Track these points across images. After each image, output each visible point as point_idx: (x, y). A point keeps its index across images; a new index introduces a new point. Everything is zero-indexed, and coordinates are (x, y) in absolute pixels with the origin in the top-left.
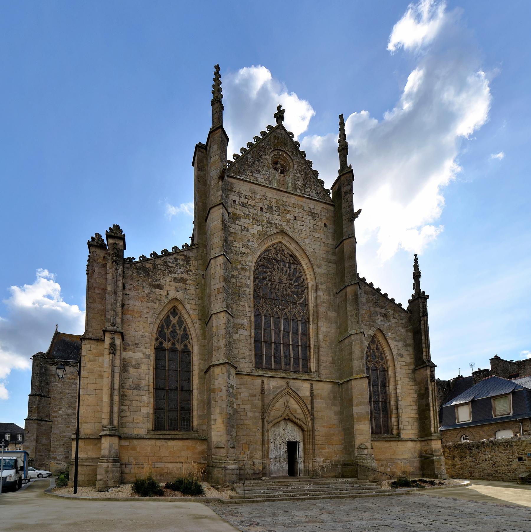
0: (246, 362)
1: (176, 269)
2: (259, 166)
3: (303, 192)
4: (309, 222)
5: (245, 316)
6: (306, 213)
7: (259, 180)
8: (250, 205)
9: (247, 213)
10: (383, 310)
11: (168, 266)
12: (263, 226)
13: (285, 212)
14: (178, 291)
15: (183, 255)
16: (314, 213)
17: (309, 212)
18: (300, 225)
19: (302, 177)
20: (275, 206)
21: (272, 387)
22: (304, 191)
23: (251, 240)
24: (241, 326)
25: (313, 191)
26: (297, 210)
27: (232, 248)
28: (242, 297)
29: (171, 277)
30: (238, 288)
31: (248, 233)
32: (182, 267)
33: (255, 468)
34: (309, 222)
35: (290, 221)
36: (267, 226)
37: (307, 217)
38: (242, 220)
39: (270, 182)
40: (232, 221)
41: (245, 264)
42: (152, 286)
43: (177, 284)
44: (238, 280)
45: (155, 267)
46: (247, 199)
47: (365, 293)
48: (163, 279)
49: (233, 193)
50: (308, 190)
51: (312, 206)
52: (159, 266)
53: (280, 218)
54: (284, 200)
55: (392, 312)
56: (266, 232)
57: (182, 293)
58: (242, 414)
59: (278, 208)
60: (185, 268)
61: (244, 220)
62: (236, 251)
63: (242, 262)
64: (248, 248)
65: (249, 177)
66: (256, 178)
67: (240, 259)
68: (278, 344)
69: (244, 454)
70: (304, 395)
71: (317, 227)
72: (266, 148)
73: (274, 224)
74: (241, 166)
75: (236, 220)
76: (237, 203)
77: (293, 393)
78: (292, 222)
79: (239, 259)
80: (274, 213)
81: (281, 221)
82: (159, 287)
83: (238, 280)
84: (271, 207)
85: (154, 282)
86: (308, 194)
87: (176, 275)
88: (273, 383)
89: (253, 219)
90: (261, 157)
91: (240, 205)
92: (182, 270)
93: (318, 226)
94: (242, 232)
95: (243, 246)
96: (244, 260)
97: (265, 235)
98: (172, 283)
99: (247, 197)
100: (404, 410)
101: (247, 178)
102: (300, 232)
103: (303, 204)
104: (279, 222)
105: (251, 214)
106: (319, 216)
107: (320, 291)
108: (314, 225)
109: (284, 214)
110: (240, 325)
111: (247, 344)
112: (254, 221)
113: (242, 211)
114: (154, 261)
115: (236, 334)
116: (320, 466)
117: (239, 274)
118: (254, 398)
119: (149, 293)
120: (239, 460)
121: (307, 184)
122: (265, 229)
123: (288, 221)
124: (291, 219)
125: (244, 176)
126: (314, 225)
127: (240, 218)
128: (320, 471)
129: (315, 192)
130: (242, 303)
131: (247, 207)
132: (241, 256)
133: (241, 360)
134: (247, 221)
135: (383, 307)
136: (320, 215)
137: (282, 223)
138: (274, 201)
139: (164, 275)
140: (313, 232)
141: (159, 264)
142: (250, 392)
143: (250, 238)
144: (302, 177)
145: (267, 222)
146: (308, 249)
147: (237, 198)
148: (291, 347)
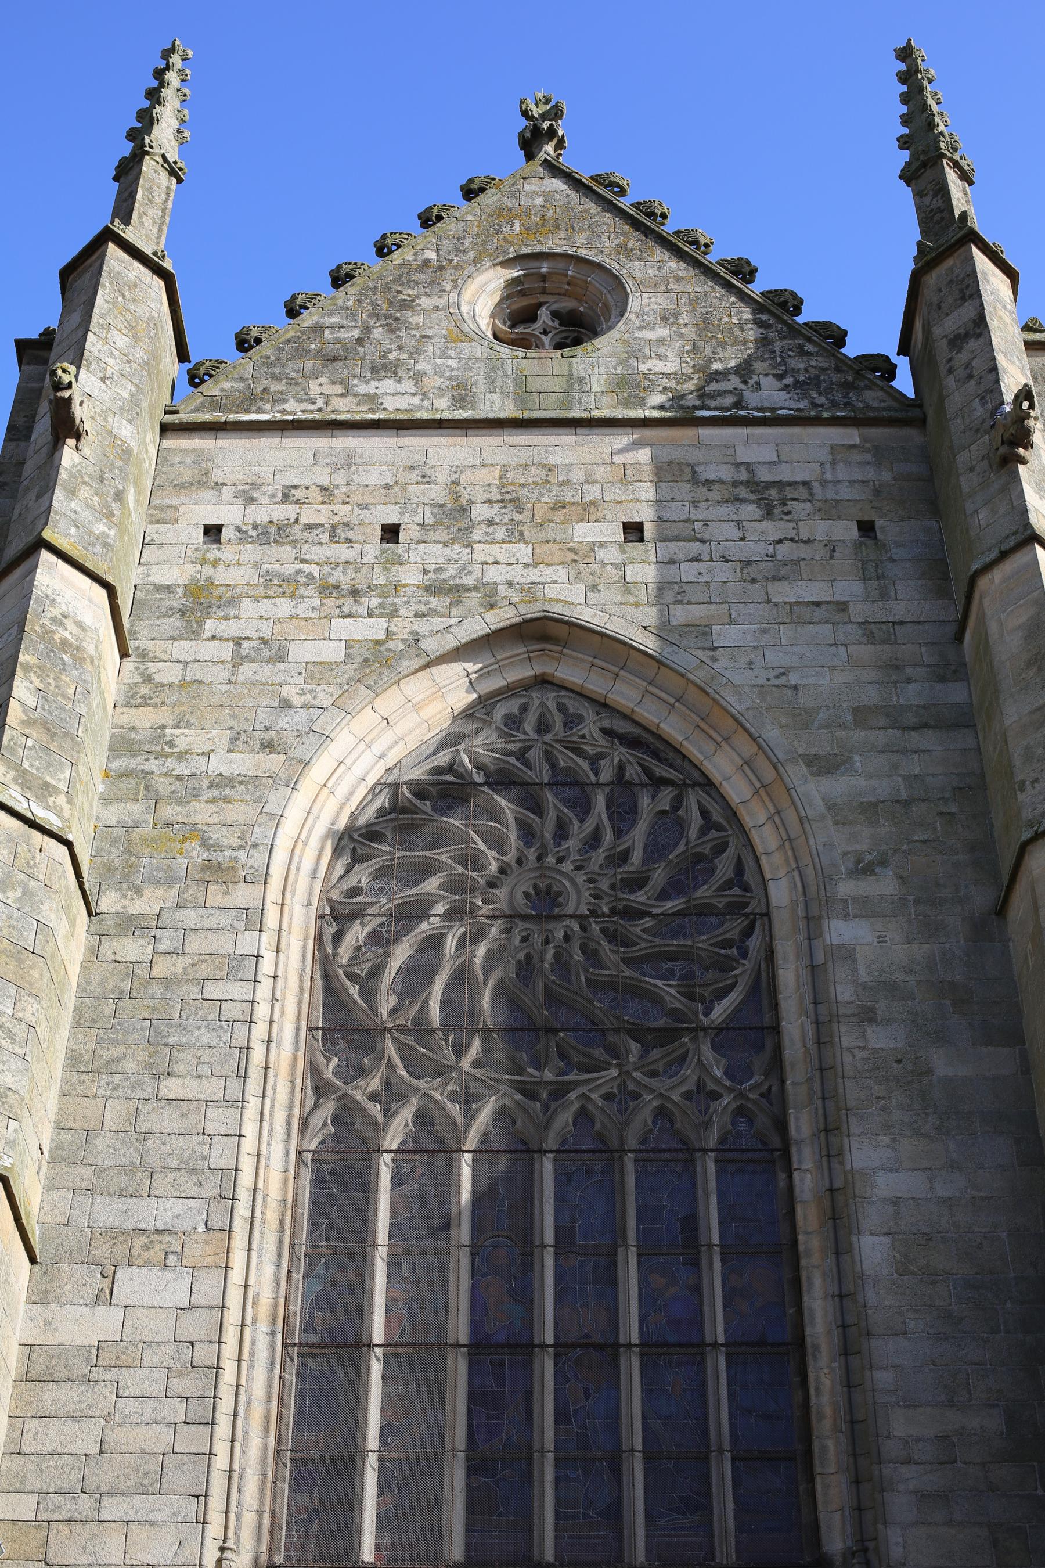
0: (158, 1517)
2: (394, 346)
4: (736, 534)
5: (193, 1172)
6: (715, 495)
7: (390, 403)
8: (310, 527)
9: (289, 569)
12: (393, 614)
13: (559, 515)
16: (780, 485)
17: (736, 484)
20: (489, 502)
23: (297, 701)
24: (146, 1248)
25: (768, 382)
27: (153, 765)
30: (157, 990)
31: (282, 666)
34: (736, 534)
35: (600, 554)
36: (423, 608)
37: (725, 510)
40: (174, 628)
41: (236, 842)
44: (165, 945)
46: (297, 502)
49: (209, 494)
53: (524, 552)
54: (556, 458)
56: (417, 638)
61: (265, 607)
62: (179, 778)
63: (217, 835)
64: (269, 746)
65: (320, 403)
67: (202, 813)
71: (803, 551)
72: (441, 268)
73: (476, 588)
74: (276, 370)
78: (611, 555)
79: (198, 819)
80: (477, 534)
81: (526, 565)
83: (165, 945)
84: (463, 510)
86: (729, 401)
89: (327, 589)
93: (808, 542)
95: (234, 740)
96: (230, 819)
99: (299, 494)
103: (694, 456)
104: (517, 574)
107: (846, 917)
108: (780, 541)
110: (139, 1243)
111: (182, 1372)
112: (330, 602)
113: (257, 565)
115: (101, 1310)
122: (403, 627)
124: (602, 545)
125: (291, 405)
126: (780, 541)
127: (234, 601)
129: (779, 385)
130: (172, 1087)
131: (294, 543)
133: (113, 1509)
134: (284, 607)
136: (823, 483)
137: (533, 575)
140: (776, 578)
143: (289, 692)
145: (427, 589)
148: (632, 1367)
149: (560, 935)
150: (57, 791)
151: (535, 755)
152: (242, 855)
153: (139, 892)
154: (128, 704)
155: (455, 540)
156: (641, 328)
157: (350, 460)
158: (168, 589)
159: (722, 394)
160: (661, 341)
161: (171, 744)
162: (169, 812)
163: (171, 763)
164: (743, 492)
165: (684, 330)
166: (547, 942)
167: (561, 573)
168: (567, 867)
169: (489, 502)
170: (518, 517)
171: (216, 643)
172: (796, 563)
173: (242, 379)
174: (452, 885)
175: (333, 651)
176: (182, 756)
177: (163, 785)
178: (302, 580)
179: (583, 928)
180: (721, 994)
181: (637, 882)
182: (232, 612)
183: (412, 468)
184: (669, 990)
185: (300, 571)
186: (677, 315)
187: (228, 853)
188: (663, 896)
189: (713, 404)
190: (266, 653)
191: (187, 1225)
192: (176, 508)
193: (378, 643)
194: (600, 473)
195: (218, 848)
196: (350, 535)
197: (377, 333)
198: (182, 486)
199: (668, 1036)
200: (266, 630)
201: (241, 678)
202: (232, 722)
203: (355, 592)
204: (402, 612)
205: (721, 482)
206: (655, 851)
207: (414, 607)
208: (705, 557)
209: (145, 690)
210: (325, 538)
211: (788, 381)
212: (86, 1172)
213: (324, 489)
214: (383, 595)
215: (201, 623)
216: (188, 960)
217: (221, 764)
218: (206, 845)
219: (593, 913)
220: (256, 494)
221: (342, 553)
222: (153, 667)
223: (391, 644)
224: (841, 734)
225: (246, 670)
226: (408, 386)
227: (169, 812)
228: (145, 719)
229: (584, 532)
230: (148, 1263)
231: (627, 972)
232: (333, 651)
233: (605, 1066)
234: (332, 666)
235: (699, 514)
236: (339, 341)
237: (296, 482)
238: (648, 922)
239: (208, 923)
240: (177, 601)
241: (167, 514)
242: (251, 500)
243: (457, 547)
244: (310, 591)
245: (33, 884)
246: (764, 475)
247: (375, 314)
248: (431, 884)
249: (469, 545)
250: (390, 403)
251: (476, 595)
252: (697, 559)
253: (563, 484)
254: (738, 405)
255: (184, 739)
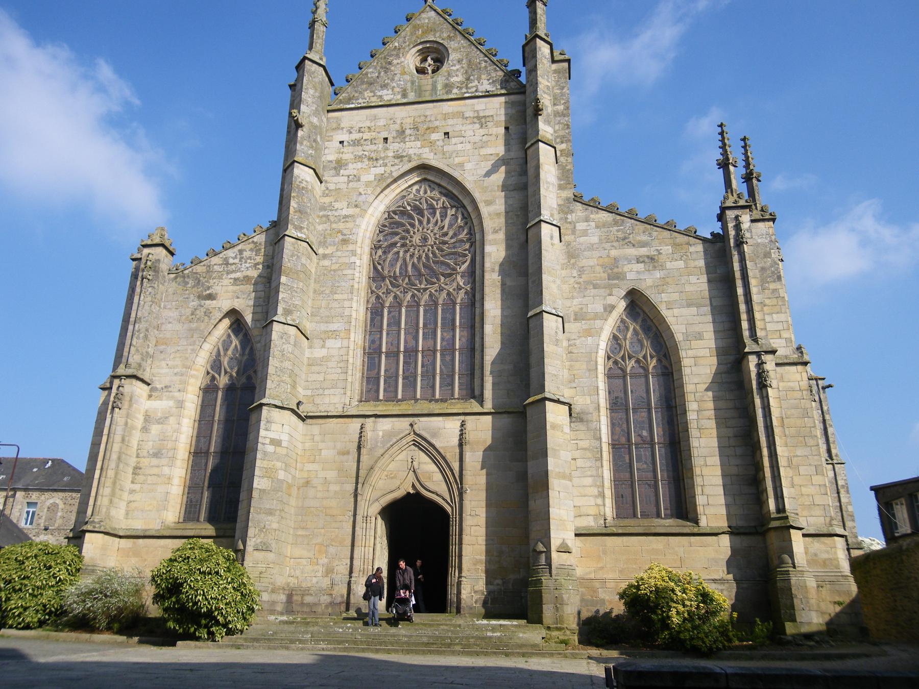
1: (239, 265)
3: (464, 90)
5: (342, 317)
6: (468, 122)
8: (366, 140)
9: (360, 153)
10: (644, 251)
11: (227, 264)
12: (386, 165)
14: (238, 298)
15: (253, 242)
16: (485, 117)
17: (474, 118)
18: (456, 144)
19: (463, 67)
20: (410, 129)
21: (381, 433)
22: (467, 88)
23: (363, 193)
24: (332, 335)
25: (486, 82)
26: (450, 122)
27: (330, 213)
28: (338, 287)
29: (231, 278)
30: (332, 273)
32: (249, 261)
33: (334, 592)
36: (393, 163)
37: (470, 126)
38: (351, 166)
39: (404, 95)
42: (200, 297)
43: (238, 287)
44: (334, 261)
45: (210, 269)
47: (597, 227)
48: (218, 284)
49: (340, 131)
50: (476, 83)
51: (478, 107)
52: (215, 267)
53: (418, 144)
54: (428, 113)
55: (667, 249)
57: (244, 298)
58: (320, 488)
59: (417, 129)
60: (252, 261)
62: (336, 216)
63: (345, 232)
64: (356, 206)
65: (368, 100)
66: (381, 97)
67: (341, 226)
68: (411, 352)
69: (317, 564)
70: (446, 444)
71: (490, 138)
72: (399, 49)
74: (356, 89)
75: (341, 169)
76: (345, 143)
77: (423, 443)
78: (440, 143)
80: (407, 139)
82: (211, 297)
85: (206, 291)
86: (474, 89)
87: (238, 275)
88: (385, 425)
89: (370, 159)
90: (390, 63)
91: (349, 145)
92: (248, 265)
93: (491, 135)
94: (350, 184)
95: (348, 205)
97: (388, 178)
98: (231, 288)
99: (362, 130)
100: (707, 459)
101: (364, 103)
102: (454, 155)
103: (464, 109)
105: (365, 153)
106: (495, 118)
109: (426, 137)
110: (330, 333)
111: (340, 362)
112: (371, 163)
113: (352, 153)
114: (210, 262)
115: (323, 349)
116: (475, 592)
117: (337, 250)
118: (346, 457)
119: (195, 309)
120: (306, 575)
121: (473, 75)
122: (388, 169)
123: (432, 143)
124: (438, 140)
125: (360, 101)
127: (346, 165)
128: (476, 602)
130: (336, 297)
132: (343, 222)
133: (327, 392)
134: (359, 165)
135: (644, 245)
137: (421, 151)
138: (410, 120)
139: (220, 278)
140: (482, 147)
141: (215, 264)
142: (339, 446)
143: (361, 190)
144: (463, 67)
145: (394, 157)
146: (469, 179)
147: (345, 137)
149: (426, 250)
150: (304, 228)
151: (423, 201)
152: (351, 236)
153: (327, 248)
154: (323, 196)
155: (402, 141)
156: (452, 66)
157: (375, 118)
158: (331, 161)
159: (472, 87)
160: (457, 70)
161: (334, 207)
162: (334, 226)
163: (334, 212)
164: (475, 120)
165: (464, 66)
166: (423, 252)
167: (427, 150)
168: (429, 232)
169: (410, 129)
170: (417, 133)
171: (343, 177)
172: (487, 142)
173: (348, 93)
174: (403, 238)
175: (371, 178)
176: (336, 210)
177: (332, 219)
178: (364, 156)
179: (432, 248)
180: (463, 263)
181: (446, 234)
182: (347, 168)
183: (391, 119)
184: (451, 262)
185: (363, 154)
186: (462, 60)
187: (348, 236)
188: (452, 238)
189: (470, 91)
190: (355, 179)
191: (340, 329)
192: (332, 136)
193: (382, 174)
194: (439, 117)
195: (345, 235)
196: (375, 142)
197: (382, 73)
198: (333, 129)
199: (450, 275)
200: (355, 172)
201: (349, 187)
202: (347, 200)
203: (377, 159)
204: (388, 165)
205: (470, 117)
206: (451, 226)
207: (391, 163)
208: (464, 142)
209: (327, 192)
210: (369, 143)
211: (491, 81)
212: (318, 318)
213: (369, 128)
214: (384, 160)
215: (340, 172)
216: (339, 265)
217: (346, 212)
218: (342, 235)
219: (435, 243)
220: (352, 131)
221: (373, 147)
222: (328, 185)
223: (385, 175)
224: (494, 193)
225: (351, 184)
226: (390, 92)
227: (334, 226)
228: (327, 200)
229: (434, 136)
230: (332, 338)
231: (442, 259)
232: (371, 178)
233: (435, 283)
234: (371, 182)
235: (464, 128)
236: (372, 77)
237: (362, 126)
238: (447, 245)
239: (344, 255)
240: (334, 165)
241: (330, 138)
242: (351, 133)
243: (402, 143)
244: (366, 160)
245: (299, 254)
246: (481, 114)
247: (381, 67)
248: (397, 238)
249: (405, 143)
250: (386, 98)
251: (406, 158)
252: (462, 143)
253: (429, 121)
254: (476, 91)
255: (337, 205)
